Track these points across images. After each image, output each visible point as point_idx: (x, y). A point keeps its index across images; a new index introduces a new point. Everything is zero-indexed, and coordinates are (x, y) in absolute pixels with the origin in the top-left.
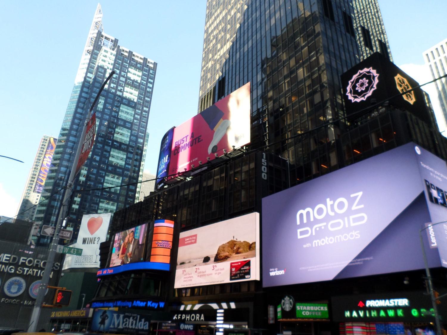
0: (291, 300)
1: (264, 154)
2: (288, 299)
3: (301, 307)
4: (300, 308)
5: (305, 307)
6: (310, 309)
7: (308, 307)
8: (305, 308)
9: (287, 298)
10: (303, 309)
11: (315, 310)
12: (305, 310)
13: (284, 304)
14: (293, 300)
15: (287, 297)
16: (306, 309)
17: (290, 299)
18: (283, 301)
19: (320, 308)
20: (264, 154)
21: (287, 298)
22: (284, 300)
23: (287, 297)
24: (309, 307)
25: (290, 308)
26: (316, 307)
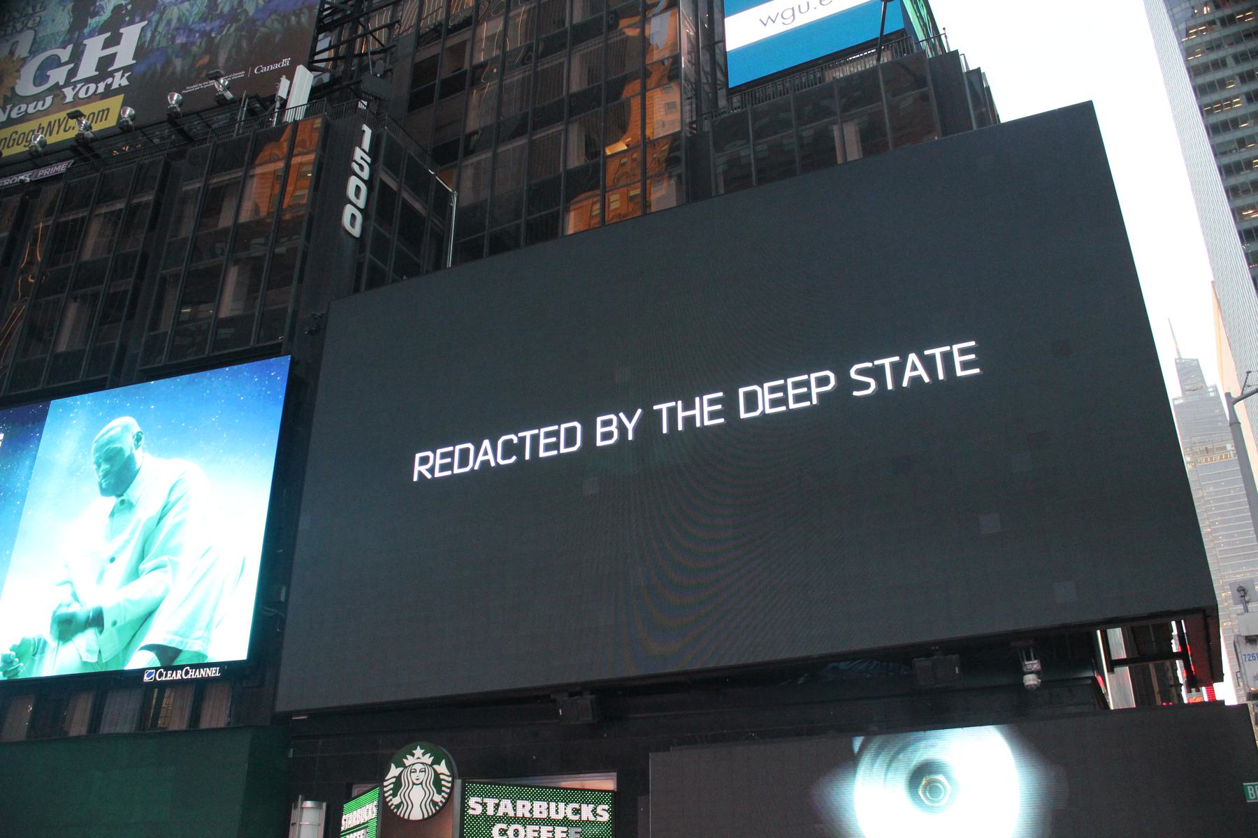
0: (442, 768)
1: (365, 128)
2: (428, 759)
3: (491, 802)
4: (484, 805)
5: (510, 806)
6: (531, 811)
7: (519, 803)
8: (506, 807)
9: (419, 758)
10: (500, 813)
11: (553, 815)
12: (507, 819)
13: (398, 784)
14: (449, 767)
15: (418, 752)
16: (511, 814)
17: (437, 761)
18: (394, 771)
19: (577, 811)
20: (365, 128)
21: (419, 758)
22: (400, 764)
23: (418, 752)
24: (528, 804)
25: (435, 803)
26: (561, 805)
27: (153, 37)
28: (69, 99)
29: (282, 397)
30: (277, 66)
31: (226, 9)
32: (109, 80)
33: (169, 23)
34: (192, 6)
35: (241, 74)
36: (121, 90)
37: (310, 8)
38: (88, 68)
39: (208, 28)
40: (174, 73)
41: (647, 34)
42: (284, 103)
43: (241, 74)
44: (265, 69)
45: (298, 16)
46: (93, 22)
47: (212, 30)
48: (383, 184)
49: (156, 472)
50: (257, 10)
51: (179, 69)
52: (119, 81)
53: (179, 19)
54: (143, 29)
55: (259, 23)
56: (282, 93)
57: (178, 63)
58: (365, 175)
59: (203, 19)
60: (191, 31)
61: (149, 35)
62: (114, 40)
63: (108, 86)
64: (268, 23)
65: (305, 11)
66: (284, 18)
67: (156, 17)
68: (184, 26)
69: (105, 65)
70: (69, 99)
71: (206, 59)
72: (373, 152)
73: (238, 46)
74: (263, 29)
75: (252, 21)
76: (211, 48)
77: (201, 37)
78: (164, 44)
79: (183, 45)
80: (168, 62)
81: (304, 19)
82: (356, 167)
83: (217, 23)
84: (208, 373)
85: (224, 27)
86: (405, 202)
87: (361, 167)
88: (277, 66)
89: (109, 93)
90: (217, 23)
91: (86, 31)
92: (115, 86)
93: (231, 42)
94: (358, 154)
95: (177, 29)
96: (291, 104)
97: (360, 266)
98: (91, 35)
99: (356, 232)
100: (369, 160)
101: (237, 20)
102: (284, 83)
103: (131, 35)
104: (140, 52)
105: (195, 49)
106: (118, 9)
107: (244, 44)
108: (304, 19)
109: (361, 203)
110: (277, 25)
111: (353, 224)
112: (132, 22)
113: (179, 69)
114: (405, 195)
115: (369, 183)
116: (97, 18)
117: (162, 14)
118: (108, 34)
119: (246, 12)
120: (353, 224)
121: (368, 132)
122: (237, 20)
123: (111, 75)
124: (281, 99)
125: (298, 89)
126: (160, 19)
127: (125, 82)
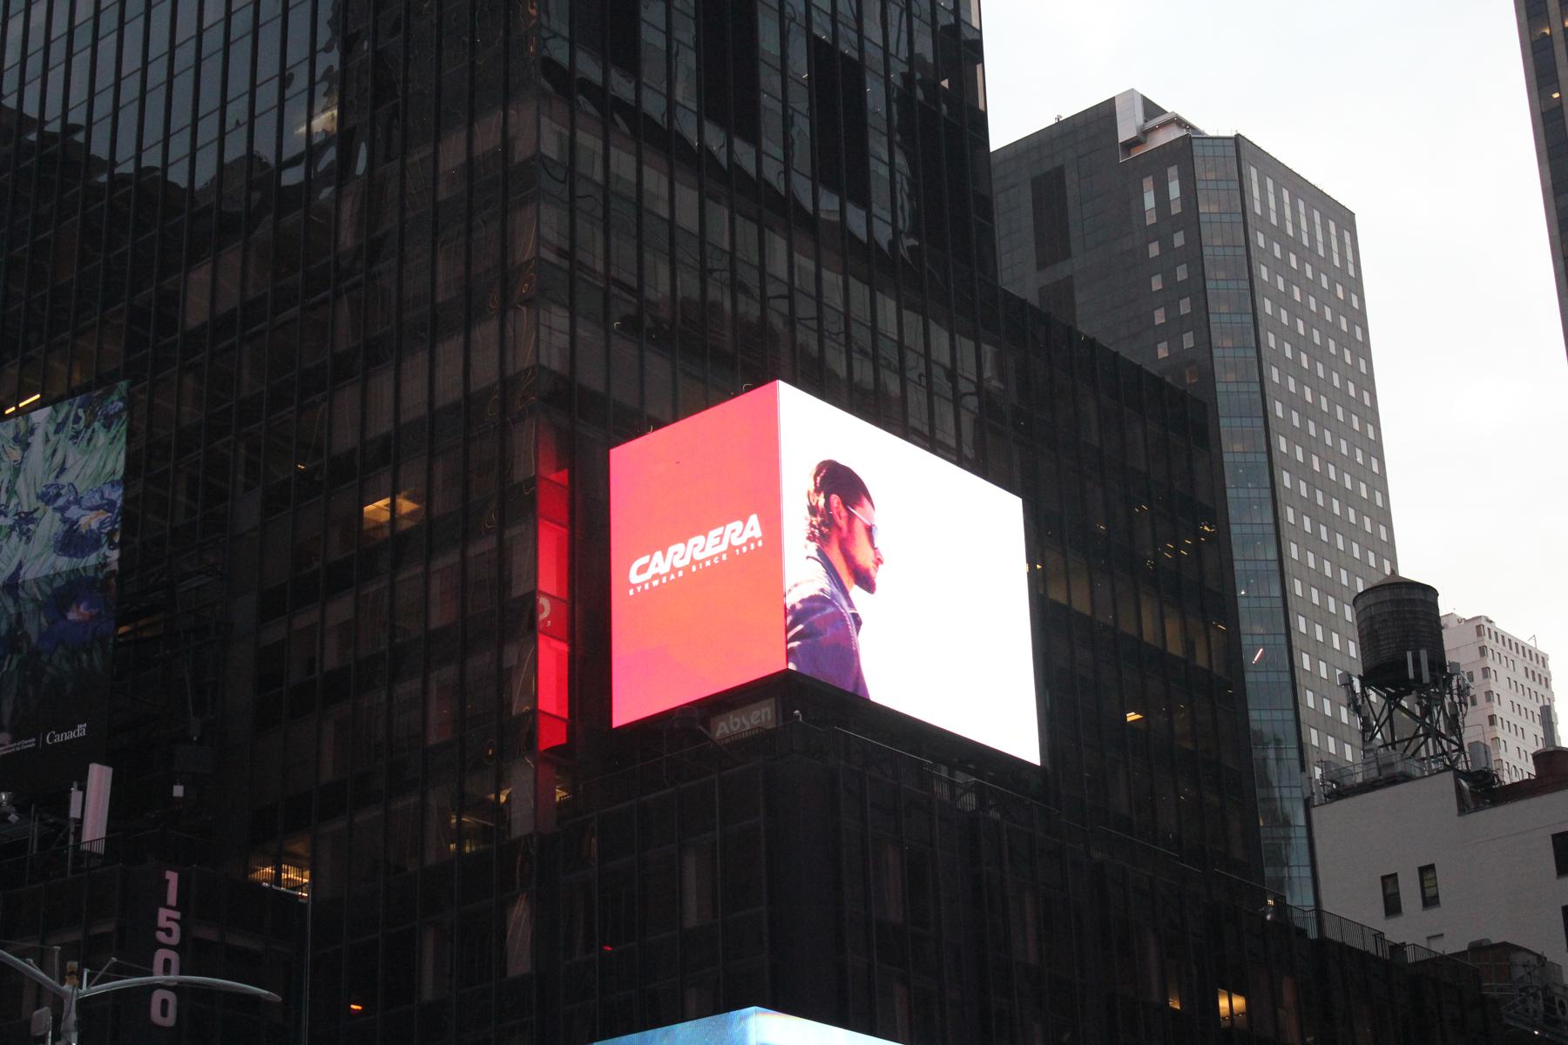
30: (72, 735)
35: (30, 743)
42: (80, 821)
43: (30, 743)
44: (59, 738)
55: (45, 658)
56: (75, 812)
58: (175, 939)
82: (161, 936)
87: (169, 932)
88: (72, 735)
94: (163, 913)
99: (170, 1021)
102: (76, 796)
111: (164, 1013)
119: (26, 635)
120: (164, 1013)
121: (172, 877)
124: (75, 819)
125: (93, 802)
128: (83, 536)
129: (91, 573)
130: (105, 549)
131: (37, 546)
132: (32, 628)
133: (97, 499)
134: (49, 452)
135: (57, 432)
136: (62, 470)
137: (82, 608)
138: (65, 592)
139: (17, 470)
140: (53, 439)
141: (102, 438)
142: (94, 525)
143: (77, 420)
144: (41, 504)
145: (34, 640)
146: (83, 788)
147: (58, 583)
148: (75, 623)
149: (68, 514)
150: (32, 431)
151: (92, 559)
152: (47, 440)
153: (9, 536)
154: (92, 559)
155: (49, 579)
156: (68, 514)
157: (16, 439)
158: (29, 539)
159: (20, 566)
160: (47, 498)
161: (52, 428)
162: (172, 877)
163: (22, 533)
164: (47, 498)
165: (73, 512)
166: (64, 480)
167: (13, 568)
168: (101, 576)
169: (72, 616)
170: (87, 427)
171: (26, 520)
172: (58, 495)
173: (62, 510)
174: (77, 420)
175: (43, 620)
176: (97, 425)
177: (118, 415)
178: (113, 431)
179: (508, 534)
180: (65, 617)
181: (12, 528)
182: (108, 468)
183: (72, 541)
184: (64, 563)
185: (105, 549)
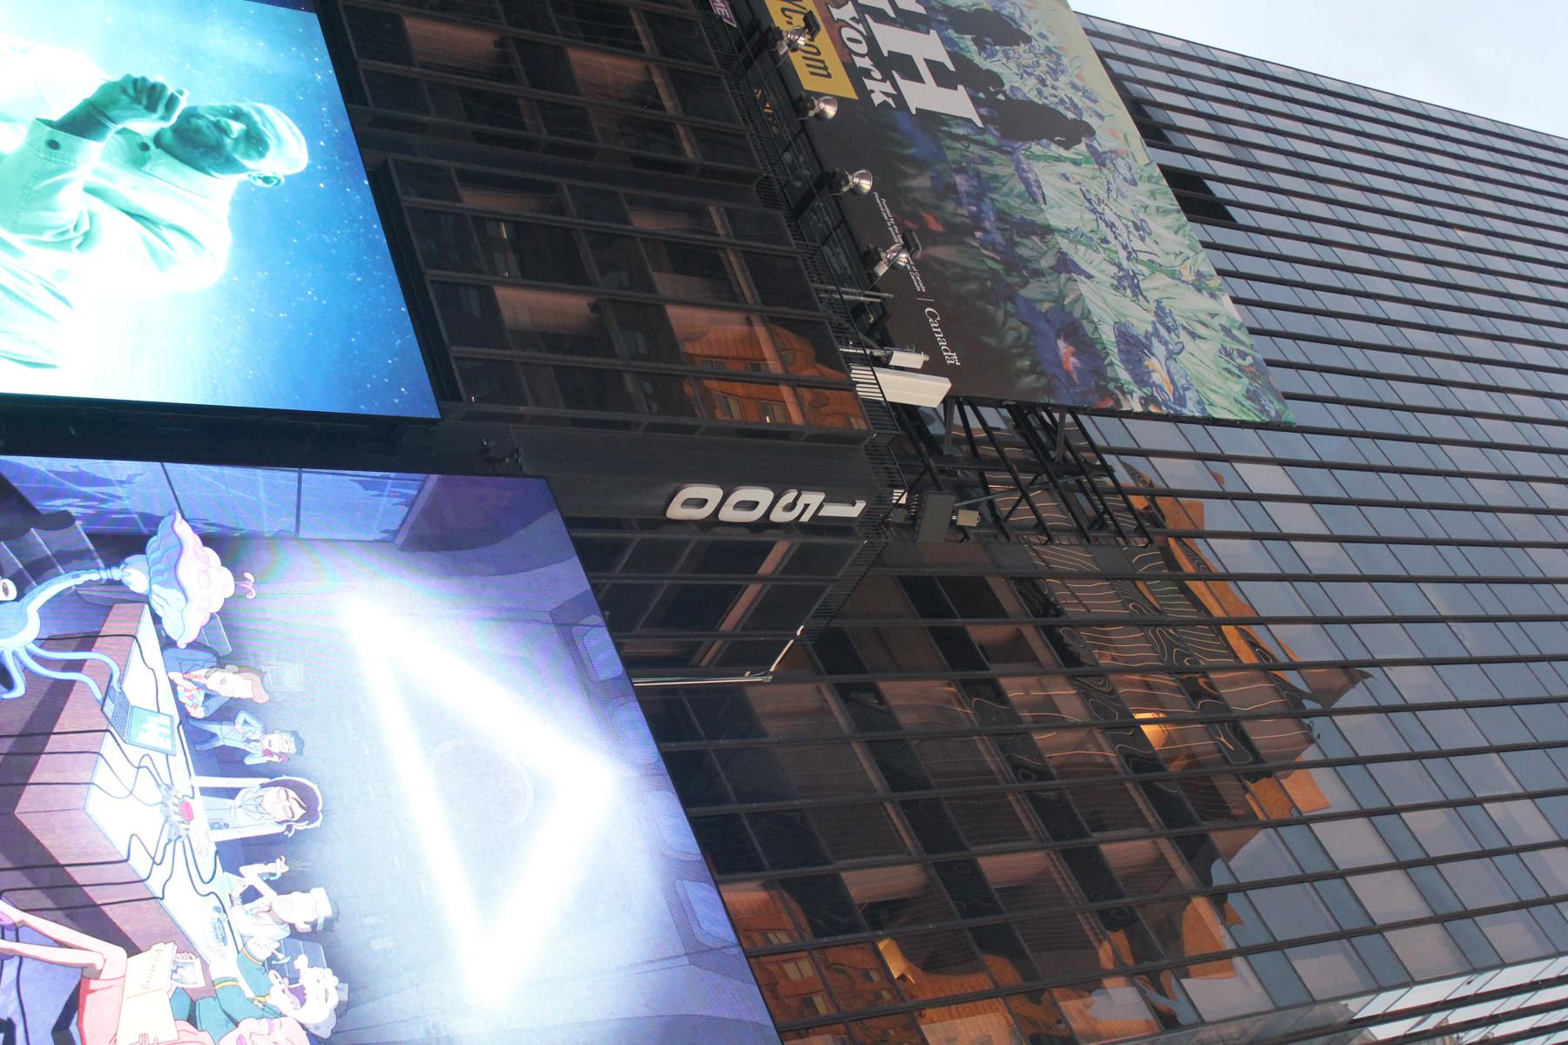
1: (860, 505)
20: (860, 505)
27: (958, 138)
28: (837, 13)
29: (363, 409)
30: (943, 344)
31: (1023, 252)
32: (876, 74)
33: (985, 161)
34: (1019, 196)
35: (920, 287)
36: (865, 93)
37: (1048, 389)
38: (892, 39)
39: (987, 224)
40: (906, 176)
41: (1107, 982)
42: (883, 363)
43: (920, 287)
44: (934, 324)
45: (1032, 370)
46: (967, 42)
47: (985, 231)
48: (766, 549)
49: (205, 201)
50: (1030, 303)
51: (914, 183)
52: (879, 91)
53: (995, 177)
54: (970, 121)
55: (1010, 306)
56: (899, 358)
57: (921, 182)
58: (779, 516)
59: (1002, 216)
60: (978, 197)
61: (961, 131)
62: (942, 77)
63: (867, 73)
64: (1013, 322)
65: (1043, 381)
66: (1025, 348)
67: (993, 141)
68: (985, 187)
69: (901, 65)
70: (837, 13)
71: (936, 227)
72: (820, 525)
73: (966, 276)
74: (1001, 314)
75: (1012, 297)
76: (956, 233)
77: (972, 215)
78: (951, 156)
79: (953, 188)
80: (921, 165)
81: (1028, 381)
82: (789, 497)
83: (998, 237)
84: (393, 277)
85: (996, 251)
86: (737, 591)
87: (790, 507)
88: (943, 344)
89: (857, 76)
90: (998, 237)
91: (951, 33)
92: (869, 84)
93: (971, 264)
94: (813, 499)
95: (978, 175)
96: (883, 375)
97: (616, 524)
98: (946, 41)
99: (676, 511)
100: (806, 518)
101: (1008, 272)
103: (957, 103)
104: (930, 120)
105: (950, 206)
106: (996, 80)
107: (972, 286)
108: (1028, 381)
109: (728, 514)
110: (1010, 336)
111: (688, 503)
112: (976, 102)
113: (914, 183)
114: (752, 591)
115: (765, 524)
116: (974, 48)
117: (1000, 149)
118: (952, 68)
119: (1025, 283)
120: (688, 503)
121: (854, 511)
122: (1008, 272)
123: (887, 77)
124: (889, 357)
125: (909, 383)
126: (991, 148)
127: (878, 99)
128: (1140, 361)
129: (1110, 374)
130: (1138, 393)
131: (1112, 297)
132: (1032, 291)
133: (1182, 382)
134: (1204, 318)
135: (1224, 328)
136: (1193, 335)
137: (1073, 360)
138: (1074, 329)
139: (1173, 275)
140: (1215, 322)
141: (1238, 387)
142: (1156, 377)
143: (1243, 355)
144: (1153, 306)
145: (1023, 292)
146: (927, 369)
147: (1088, 328)
148: (1056, 350)
149: (1155, 341)
150: (1213, 296)
151: (1124, 376)
152: (1213, 315)
153: (1113, 263)
154: (1124, 376)
155: (1087, 314)
156: (1155, 341)
157: (1199, 274)
158: (1116, 288)
159: (1090, 277)
160: (1161, 313)
161: (1224, 321)
162: (854, 511)
163: (1120, 278)
164: (1161, 313)
165: (1159, 349)
166: (1184, 337)
167: (1084, 266)
168: (1111, 386)
169: (1061, 344)
170: (1240, 368)
171: (1128, 283)
172: (1169, 330)
173: (1157, 334)
174: (1243, 355)
175: (1046, 306)
176: (1245, 380)
177: (1263, 410)
178: (1247, 403)
179: (1239, 962)
180: (1058, 336)
181: (1119, 266)
182: (1212, 396)
183: (1133, 347)
184: (1108, 336)
185: (1138, 393)
